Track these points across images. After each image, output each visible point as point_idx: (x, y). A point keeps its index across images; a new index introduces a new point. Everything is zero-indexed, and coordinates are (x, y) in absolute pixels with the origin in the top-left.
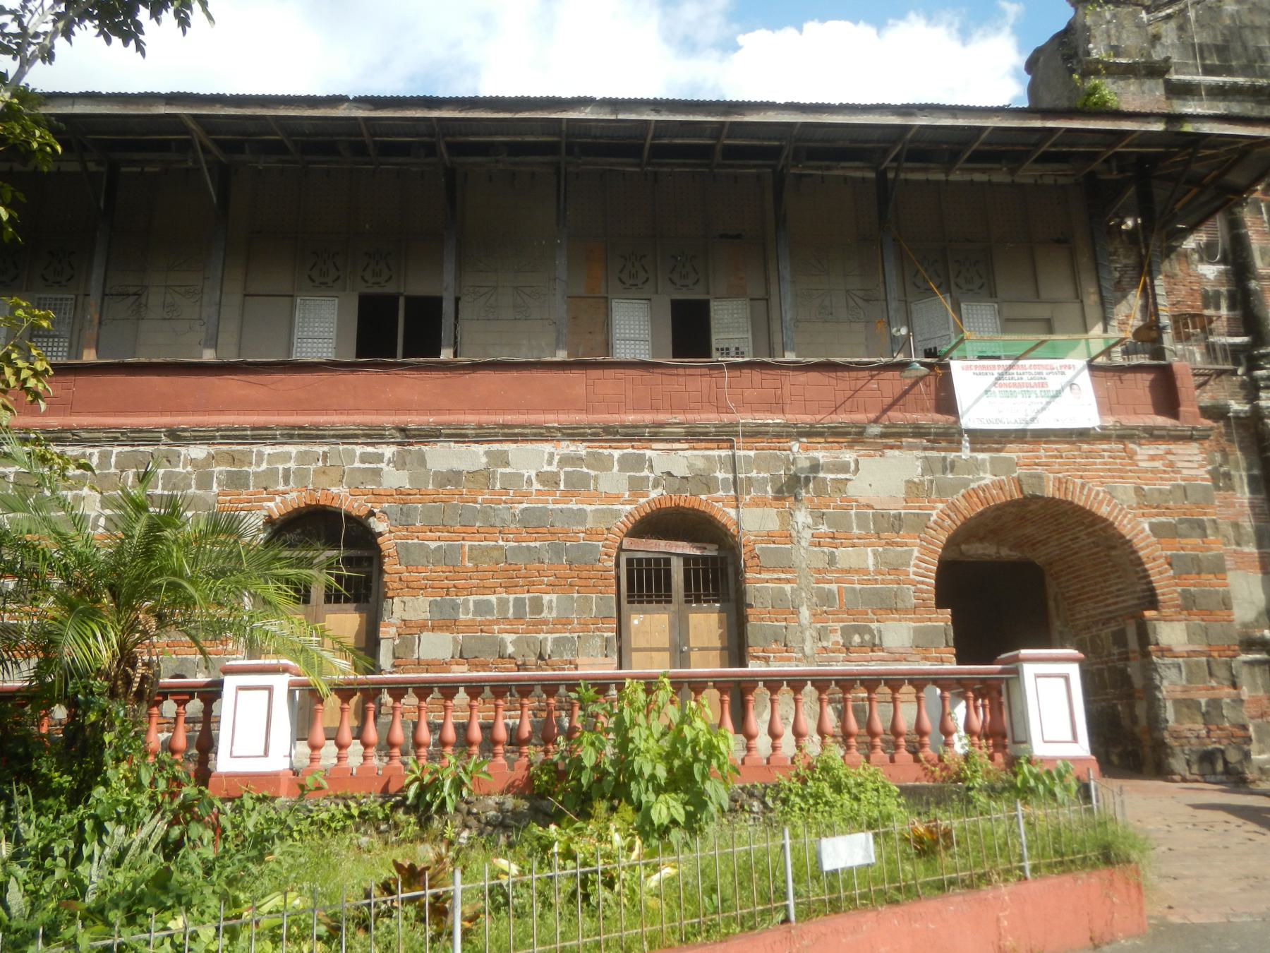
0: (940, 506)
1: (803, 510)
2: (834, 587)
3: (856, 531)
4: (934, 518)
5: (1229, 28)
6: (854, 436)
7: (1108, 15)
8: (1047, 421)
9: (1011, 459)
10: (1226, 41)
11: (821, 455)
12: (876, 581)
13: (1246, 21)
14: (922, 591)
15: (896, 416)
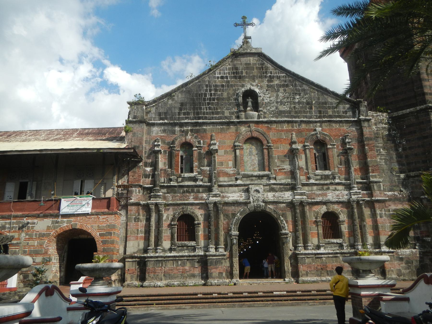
0: (54, 231)
1: (24, 233)
2: (27, 249)
3: (34, 237)
4: (52, 234)
5: (169, 108)
6: (37, 216)
7: (135, 108)
8: (80, 212)
9: (72, 220)
10: (167, 111)
11: (30, 221)
12: (36, 248)
13: (173, 106)
14: (46, 250)
15: (47, 211)
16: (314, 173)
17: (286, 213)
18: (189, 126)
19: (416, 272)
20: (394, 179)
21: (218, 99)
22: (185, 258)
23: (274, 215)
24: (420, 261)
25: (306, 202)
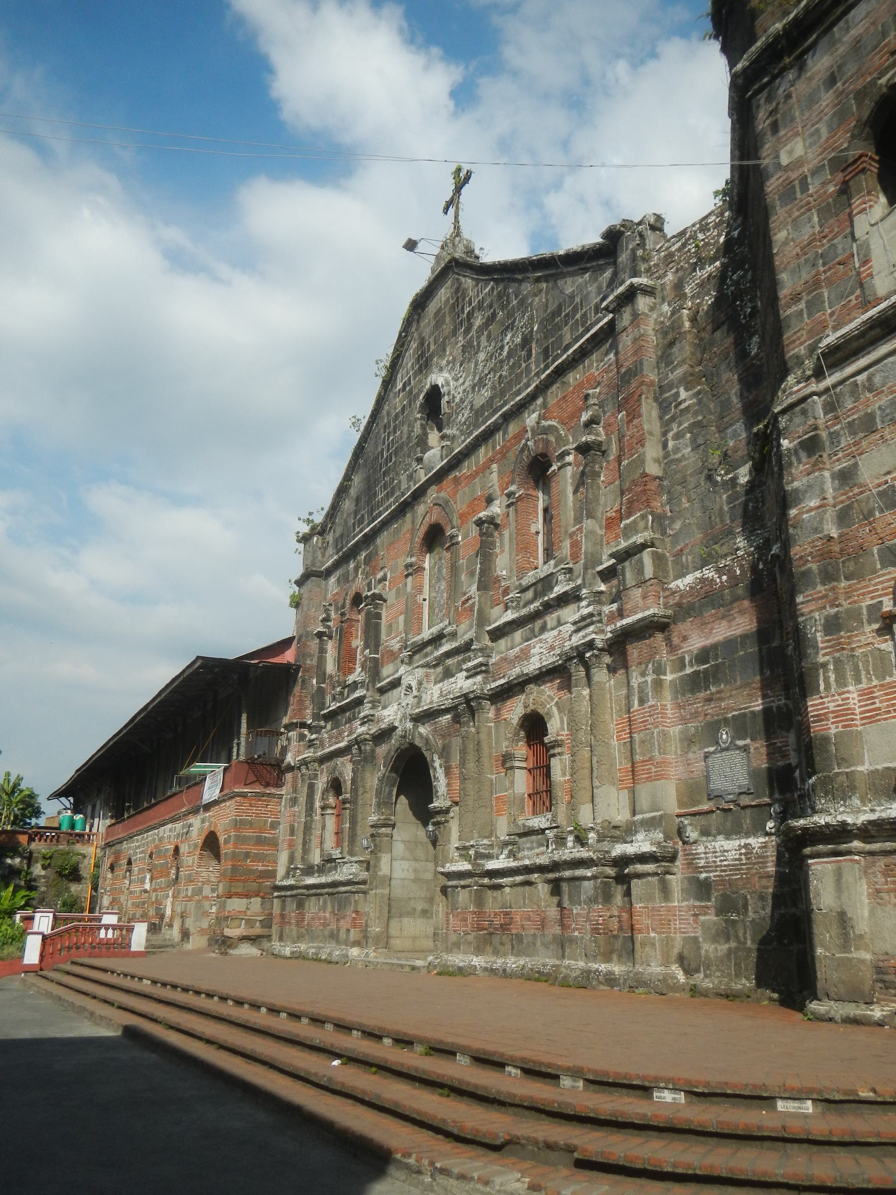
16: (520, 584)
17: (450, 742)
18: (362, 550)
19: (754, 955)
20: (717, 507)
21: (396, 453)
22: (326, 890)
23: (425, 753)
24: (778, 899)
25: (472, 696)
